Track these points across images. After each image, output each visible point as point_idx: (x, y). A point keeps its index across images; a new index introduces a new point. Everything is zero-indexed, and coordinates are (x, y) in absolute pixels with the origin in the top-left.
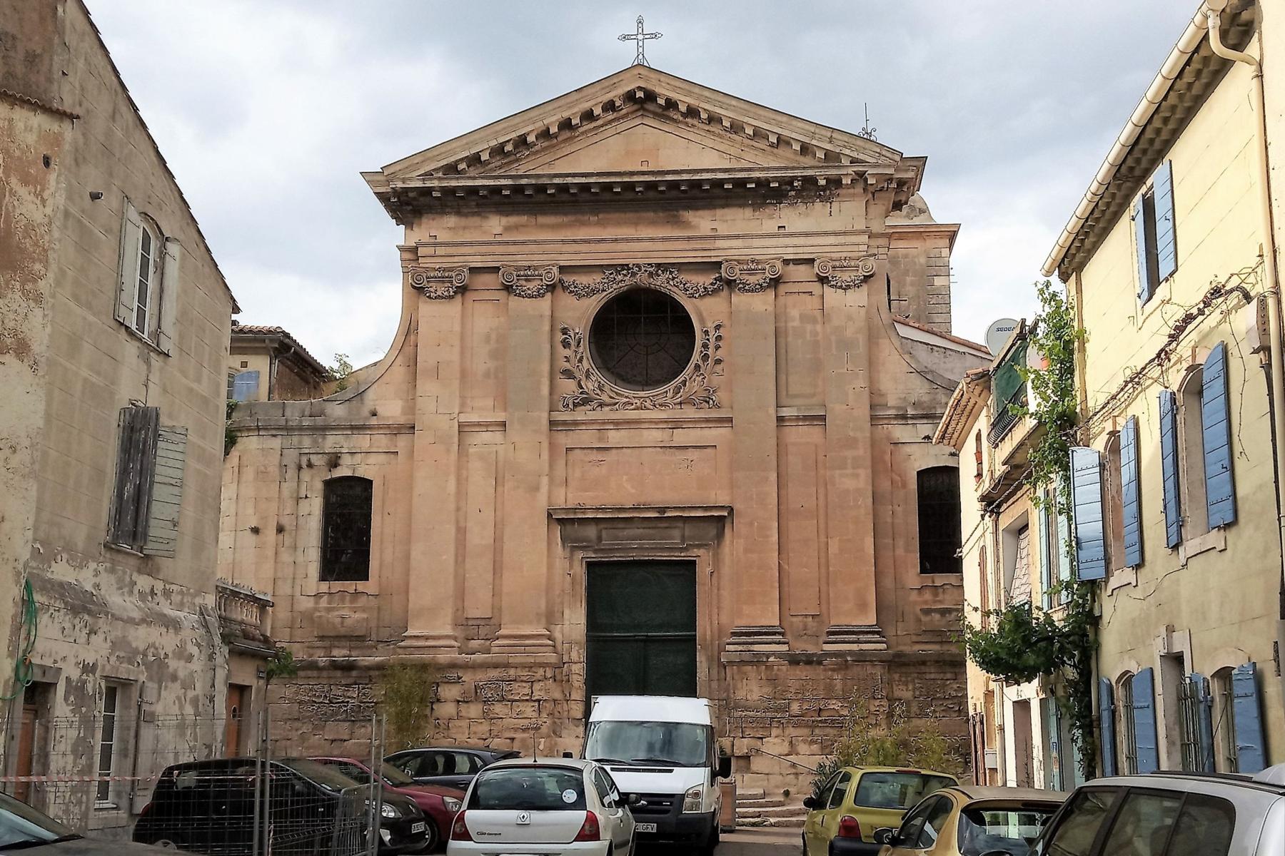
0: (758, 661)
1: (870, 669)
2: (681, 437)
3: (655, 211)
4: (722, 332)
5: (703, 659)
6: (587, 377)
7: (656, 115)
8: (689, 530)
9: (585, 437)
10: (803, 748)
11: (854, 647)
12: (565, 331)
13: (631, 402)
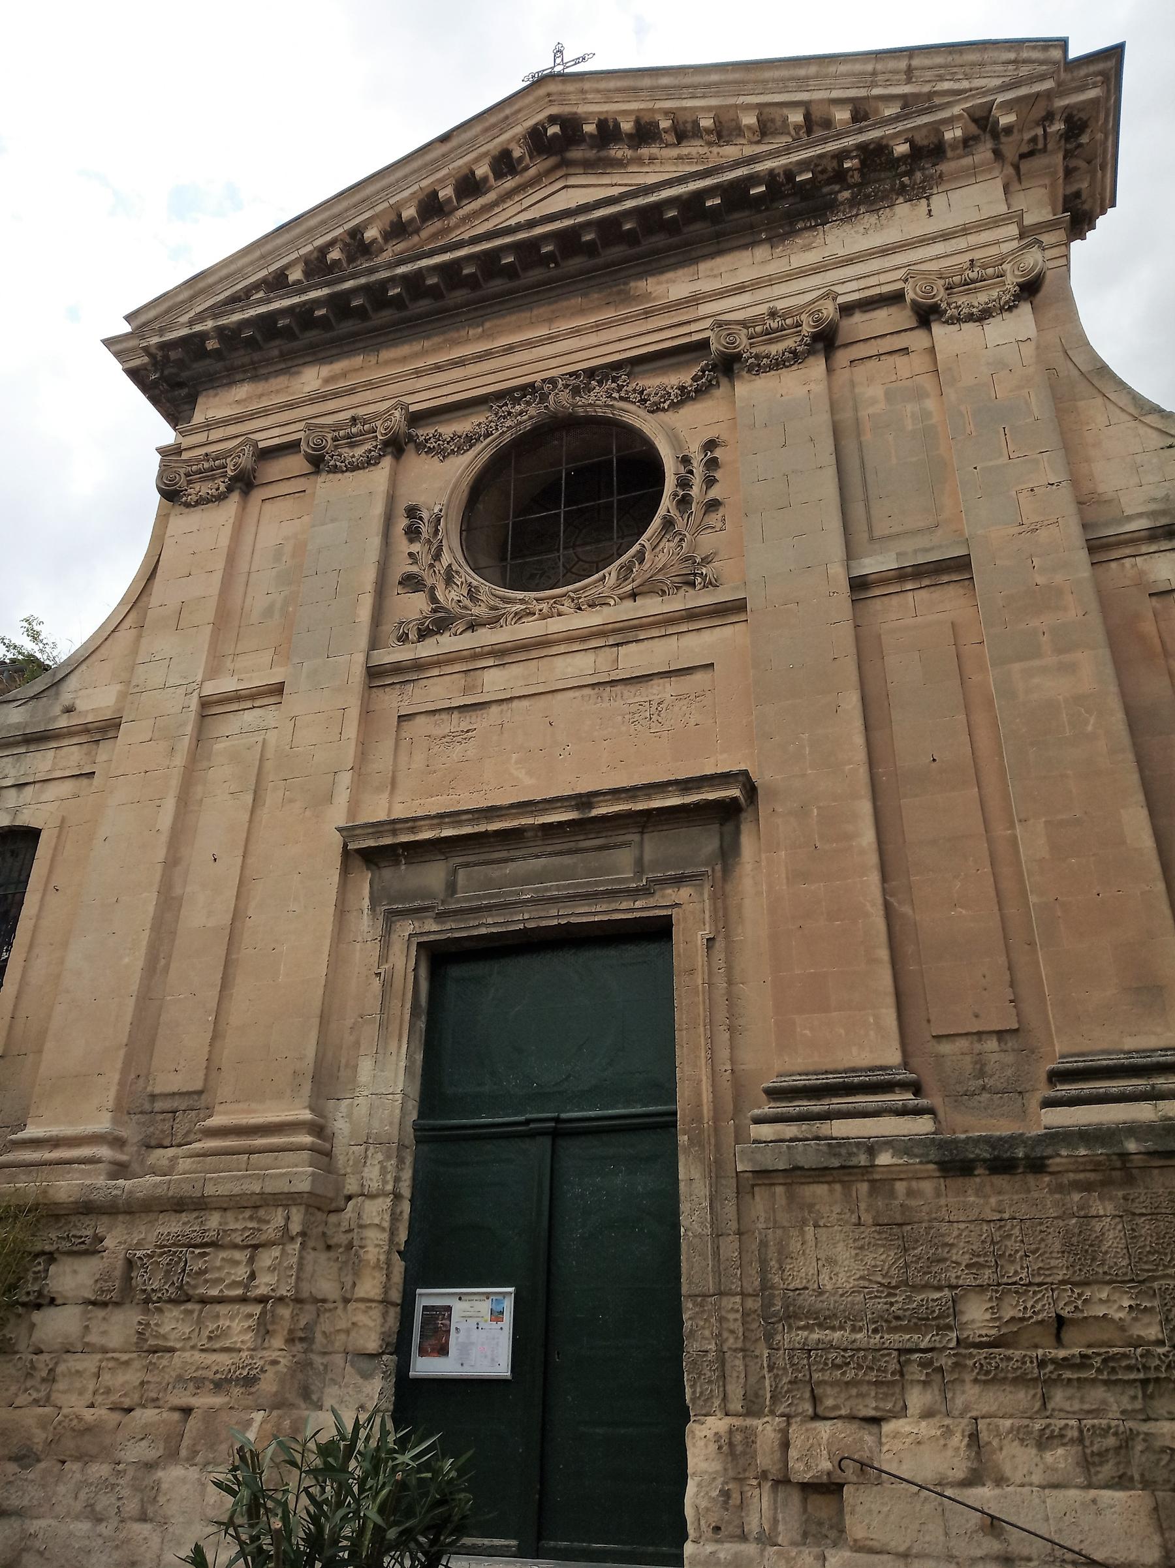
0: (844, 1168)
2: (635, 658)
4: (718, 453)
5: (696, 1174)
6: (449, 580)
8: (653, 846)
9: (439, 690)
10: (1018, 1459)
11: (1144, 1112)
12: (412, 512)
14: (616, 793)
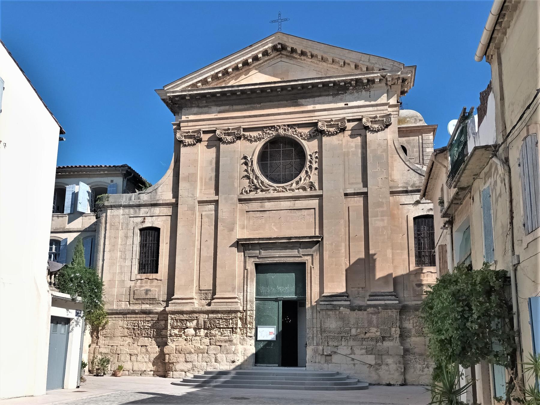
1: (389, 312)
2: (299, 204)
3: (287, 101)
7: (287, 56)
11: (382, 302)
13: (274, 189)
14: (296, 238)
